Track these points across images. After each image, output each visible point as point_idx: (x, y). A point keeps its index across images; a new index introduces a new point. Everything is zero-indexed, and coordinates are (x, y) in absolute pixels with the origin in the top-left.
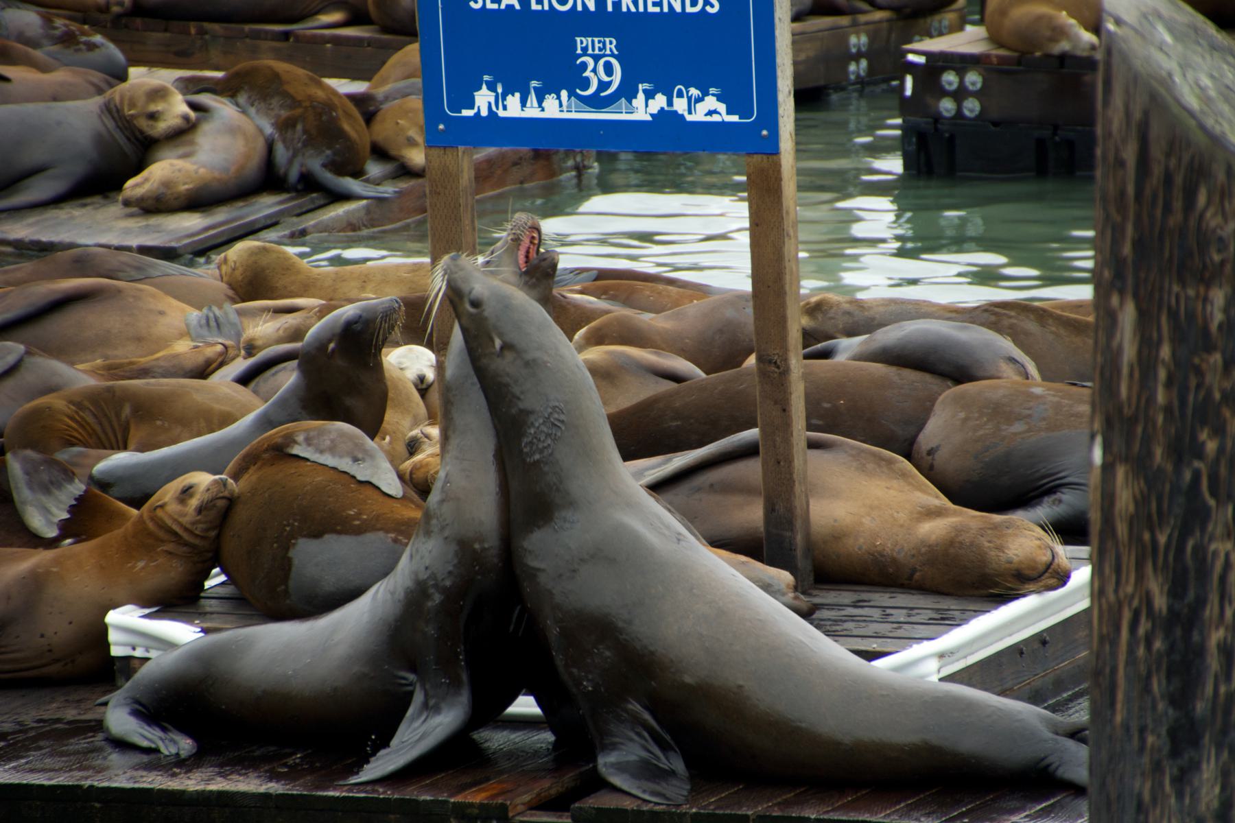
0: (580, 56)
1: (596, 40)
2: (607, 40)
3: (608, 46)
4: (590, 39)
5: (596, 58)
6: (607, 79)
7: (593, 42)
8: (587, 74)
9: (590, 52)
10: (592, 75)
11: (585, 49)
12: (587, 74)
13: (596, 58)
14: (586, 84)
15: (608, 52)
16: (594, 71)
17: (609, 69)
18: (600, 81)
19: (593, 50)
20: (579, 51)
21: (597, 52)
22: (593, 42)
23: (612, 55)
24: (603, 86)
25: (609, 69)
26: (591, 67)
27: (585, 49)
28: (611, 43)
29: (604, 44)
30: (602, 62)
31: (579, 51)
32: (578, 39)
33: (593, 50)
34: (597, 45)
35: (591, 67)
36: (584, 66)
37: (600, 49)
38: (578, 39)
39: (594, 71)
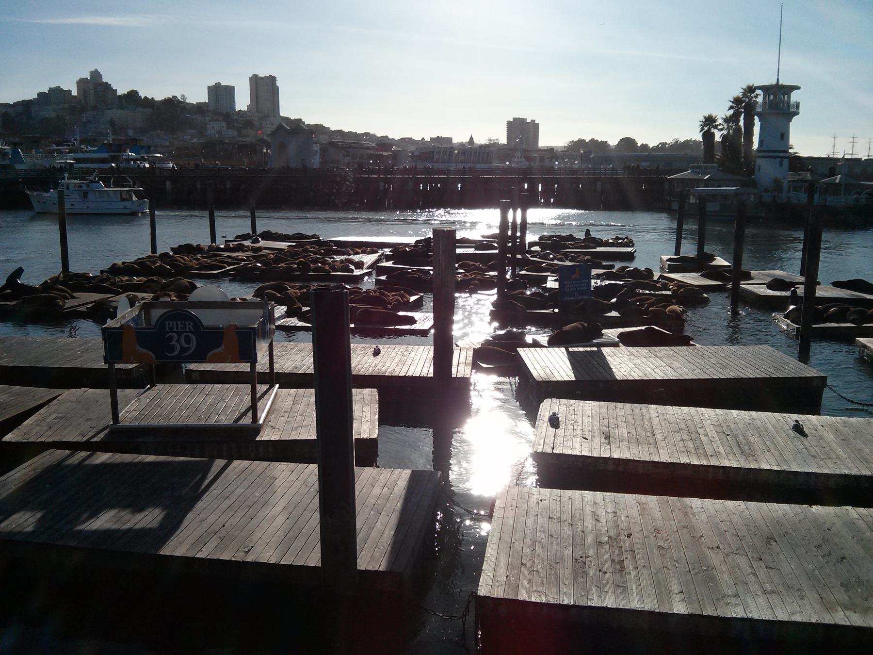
0: (168, 332)
5: (179, 334)
8: (173, 343)
12: (173, 343)
13: (179, 334)
14: (173, 348)
16: (178, 341)
17: (188, 340)
18: (182, 347)
19: (177, 328)
23: (190, 332)
24: (183, 350)
25: (188, 340)
26: (175, 340)
29: (185, 325)
30: (183, 336)
31: (167, 330)
33: (177, 328)
34: (180, 326)
35: (175, 340)
36: (171, 338)
37: (182, 328)
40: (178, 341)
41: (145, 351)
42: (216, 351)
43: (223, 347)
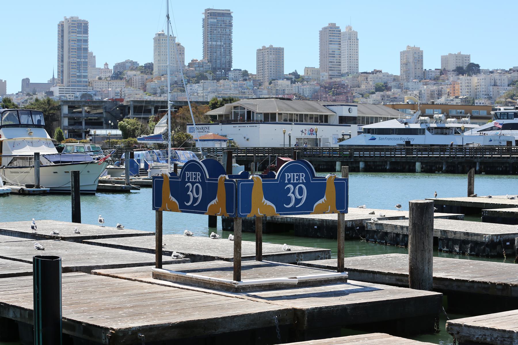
1: (295, 174)
2: (301, 174)
3: (301, 178)
4: (292, 174)
5: (295, 185)
6: (299, 197)
7: (294, 175)
8: (290, 194)
9: (292, 181)
10: (293, 195)
11: (289, 180)
13: (295, 185)
15: (301, 181)
17: (301, 192)
18: (295, 198)
19: (294, 181)
20: (286, 182)
21: (295, 181)
22: (294, 175)
23: (303, 183)
24: (298, 201)
25: (301, 192)
26: (291, 191)
27: (289, 180)
28: (303, 176)
30: (297, 187)
31: (286, 182)
32: (286, 174)
33: (294, 181)
34: (296, 177)
35: (291, 191)
36: (289, 189)
37: (297, 180)
38: (286, 174)
39: (293, 193)
40: (293, 193)
41: (269, 203)
42: (320, 202)
43: (325, 198)
